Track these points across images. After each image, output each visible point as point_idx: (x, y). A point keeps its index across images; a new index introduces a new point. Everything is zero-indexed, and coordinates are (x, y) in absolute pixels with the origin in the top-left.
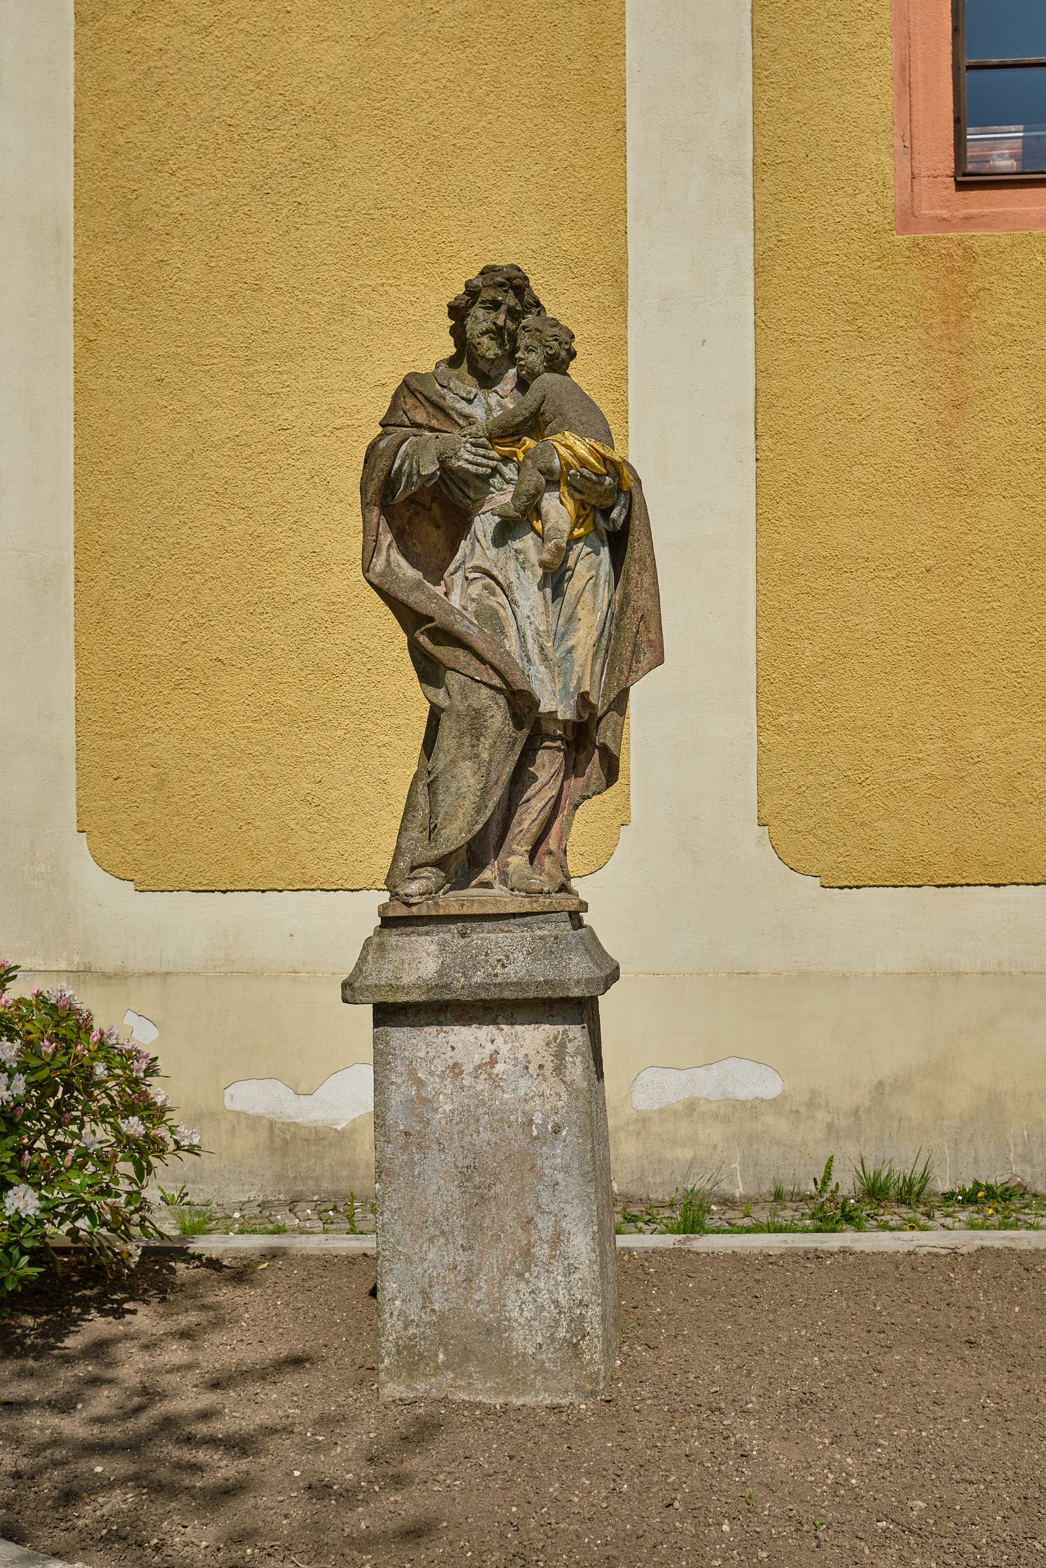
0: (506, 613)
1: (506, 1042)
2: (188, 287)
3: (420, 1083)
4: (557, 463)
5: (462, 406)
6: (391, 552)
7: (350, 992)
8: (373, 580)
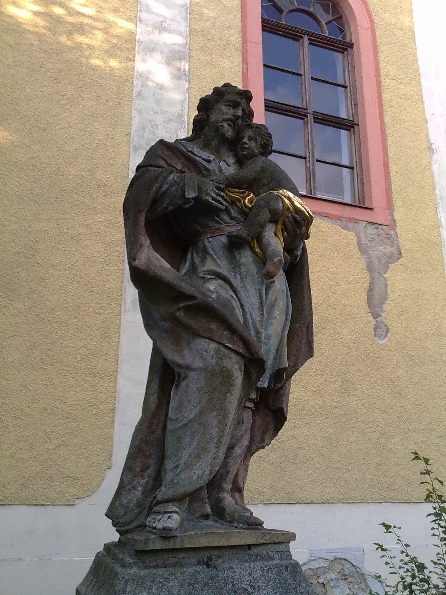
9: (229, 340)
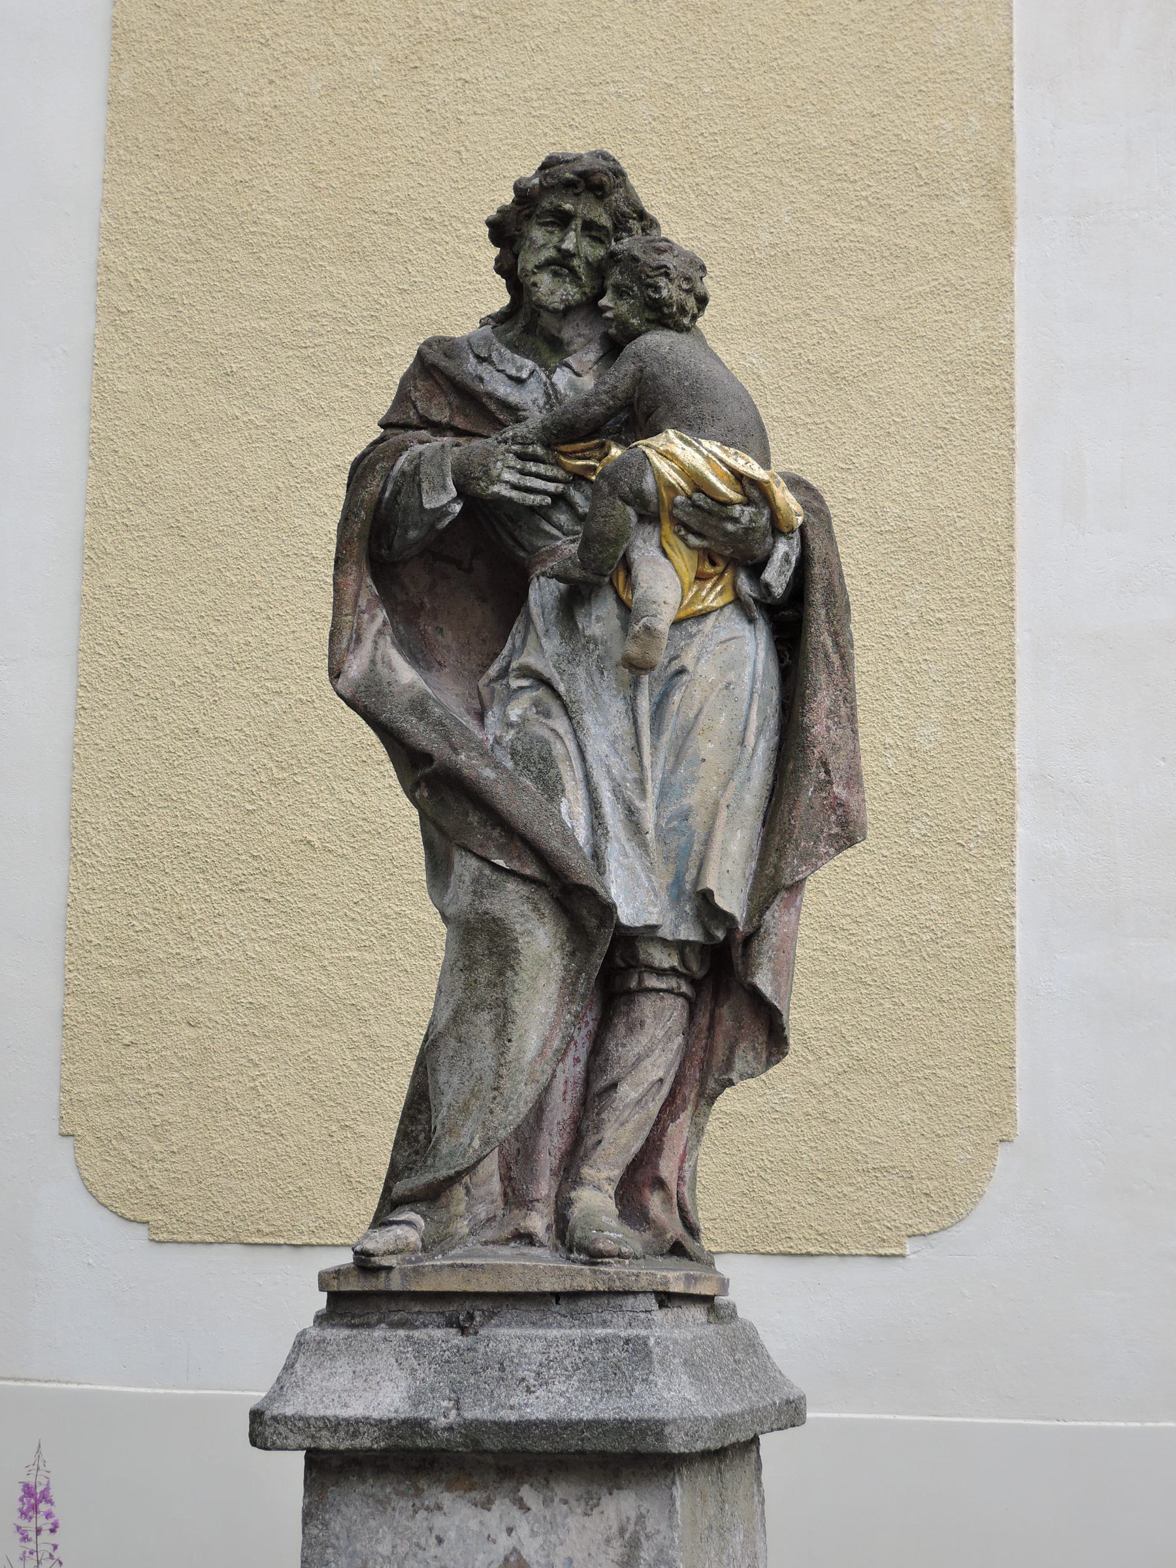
0: (563, 749)
1: (534, 1534)
2: (280, 222)
4: (649, 484)
5: (503, 389)
6: (381, 643)
7: (263, 1429)
8: (343, 692)
9: (502, 850)
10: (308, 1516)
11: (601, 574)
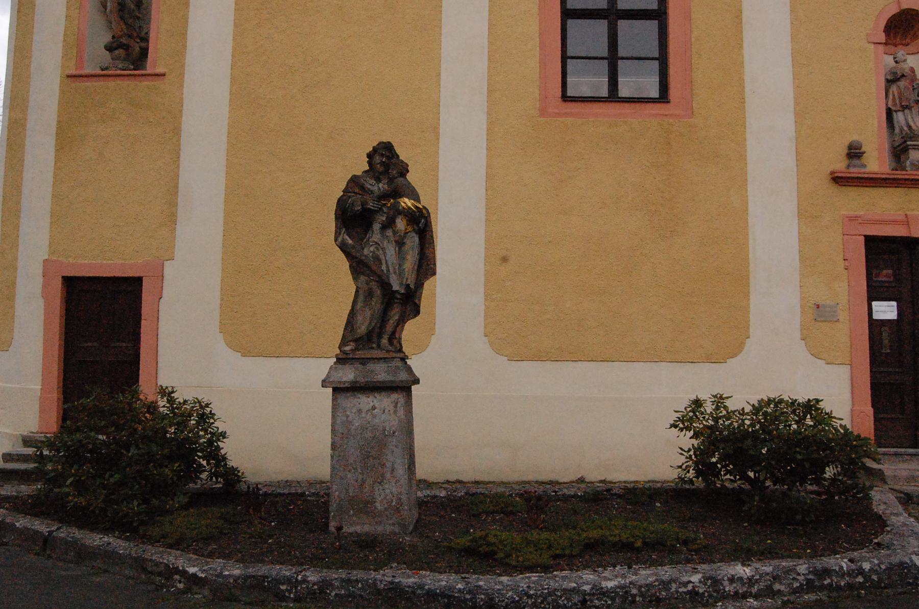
0: (382, 257)
3: (348, 416)
7: (324, 384)
10: (333, 400)
11: (389, 224)
